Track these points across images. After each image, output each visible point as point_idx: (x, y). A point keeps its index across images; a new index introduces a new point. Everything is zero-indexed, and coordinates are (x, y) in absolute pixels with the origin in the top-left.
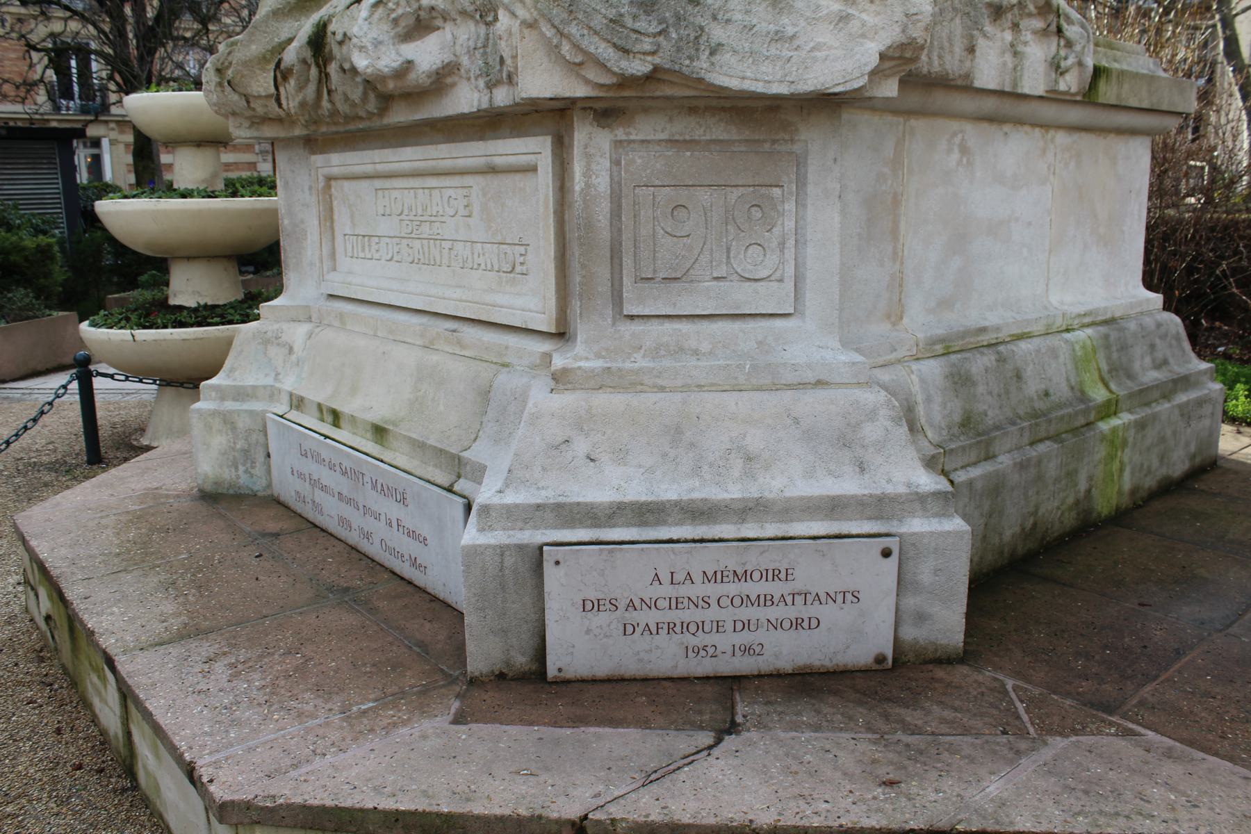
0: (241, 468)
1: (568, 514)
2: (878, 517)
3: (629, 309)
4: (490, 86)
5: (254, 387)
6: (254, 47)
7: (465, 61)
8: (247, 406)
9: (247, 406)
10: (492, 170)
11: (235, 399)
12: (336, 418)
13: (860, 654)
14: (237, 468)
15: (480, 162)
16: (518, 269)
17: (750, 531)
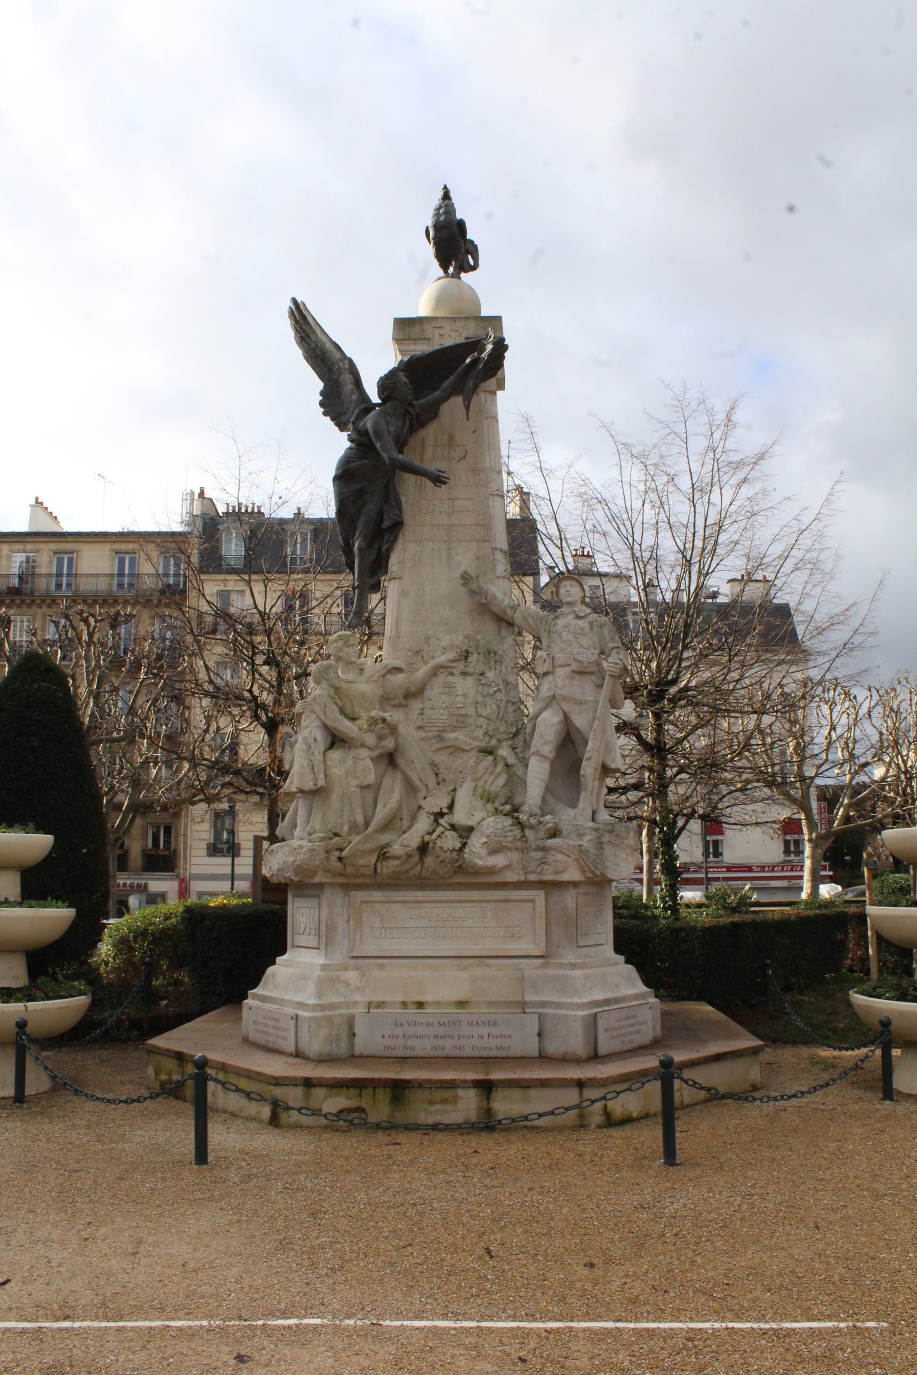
0: (334, 1045)
1: (597, 1004)
2: (643, 999)
3: (580, 944)
4: (526, 874)
5: (339, 1003)
6: (369, 845)
7: (515, 864)
8: (337, 1012)
9: (337, 1012)
10: (505, 901)
11: (329, 1010)
12: (420, 1005)
13: (648, 1041)
14: (331, 1044)
15: (501, 898)
16: (516, 935)
17: (621, 1005)
